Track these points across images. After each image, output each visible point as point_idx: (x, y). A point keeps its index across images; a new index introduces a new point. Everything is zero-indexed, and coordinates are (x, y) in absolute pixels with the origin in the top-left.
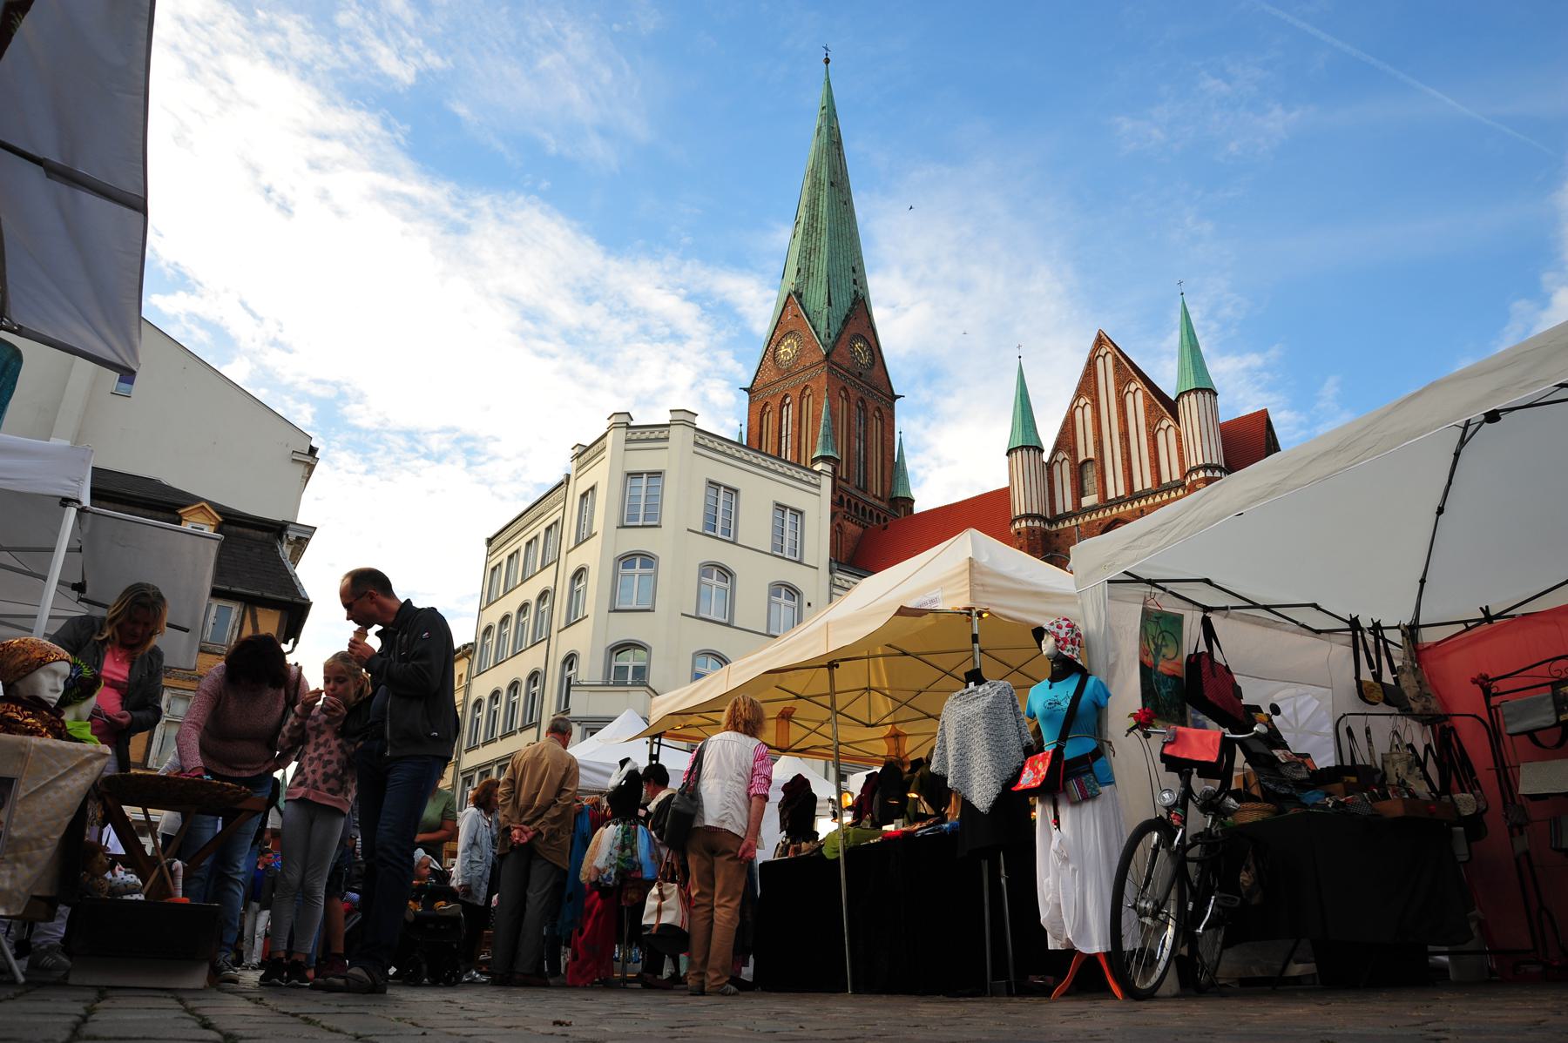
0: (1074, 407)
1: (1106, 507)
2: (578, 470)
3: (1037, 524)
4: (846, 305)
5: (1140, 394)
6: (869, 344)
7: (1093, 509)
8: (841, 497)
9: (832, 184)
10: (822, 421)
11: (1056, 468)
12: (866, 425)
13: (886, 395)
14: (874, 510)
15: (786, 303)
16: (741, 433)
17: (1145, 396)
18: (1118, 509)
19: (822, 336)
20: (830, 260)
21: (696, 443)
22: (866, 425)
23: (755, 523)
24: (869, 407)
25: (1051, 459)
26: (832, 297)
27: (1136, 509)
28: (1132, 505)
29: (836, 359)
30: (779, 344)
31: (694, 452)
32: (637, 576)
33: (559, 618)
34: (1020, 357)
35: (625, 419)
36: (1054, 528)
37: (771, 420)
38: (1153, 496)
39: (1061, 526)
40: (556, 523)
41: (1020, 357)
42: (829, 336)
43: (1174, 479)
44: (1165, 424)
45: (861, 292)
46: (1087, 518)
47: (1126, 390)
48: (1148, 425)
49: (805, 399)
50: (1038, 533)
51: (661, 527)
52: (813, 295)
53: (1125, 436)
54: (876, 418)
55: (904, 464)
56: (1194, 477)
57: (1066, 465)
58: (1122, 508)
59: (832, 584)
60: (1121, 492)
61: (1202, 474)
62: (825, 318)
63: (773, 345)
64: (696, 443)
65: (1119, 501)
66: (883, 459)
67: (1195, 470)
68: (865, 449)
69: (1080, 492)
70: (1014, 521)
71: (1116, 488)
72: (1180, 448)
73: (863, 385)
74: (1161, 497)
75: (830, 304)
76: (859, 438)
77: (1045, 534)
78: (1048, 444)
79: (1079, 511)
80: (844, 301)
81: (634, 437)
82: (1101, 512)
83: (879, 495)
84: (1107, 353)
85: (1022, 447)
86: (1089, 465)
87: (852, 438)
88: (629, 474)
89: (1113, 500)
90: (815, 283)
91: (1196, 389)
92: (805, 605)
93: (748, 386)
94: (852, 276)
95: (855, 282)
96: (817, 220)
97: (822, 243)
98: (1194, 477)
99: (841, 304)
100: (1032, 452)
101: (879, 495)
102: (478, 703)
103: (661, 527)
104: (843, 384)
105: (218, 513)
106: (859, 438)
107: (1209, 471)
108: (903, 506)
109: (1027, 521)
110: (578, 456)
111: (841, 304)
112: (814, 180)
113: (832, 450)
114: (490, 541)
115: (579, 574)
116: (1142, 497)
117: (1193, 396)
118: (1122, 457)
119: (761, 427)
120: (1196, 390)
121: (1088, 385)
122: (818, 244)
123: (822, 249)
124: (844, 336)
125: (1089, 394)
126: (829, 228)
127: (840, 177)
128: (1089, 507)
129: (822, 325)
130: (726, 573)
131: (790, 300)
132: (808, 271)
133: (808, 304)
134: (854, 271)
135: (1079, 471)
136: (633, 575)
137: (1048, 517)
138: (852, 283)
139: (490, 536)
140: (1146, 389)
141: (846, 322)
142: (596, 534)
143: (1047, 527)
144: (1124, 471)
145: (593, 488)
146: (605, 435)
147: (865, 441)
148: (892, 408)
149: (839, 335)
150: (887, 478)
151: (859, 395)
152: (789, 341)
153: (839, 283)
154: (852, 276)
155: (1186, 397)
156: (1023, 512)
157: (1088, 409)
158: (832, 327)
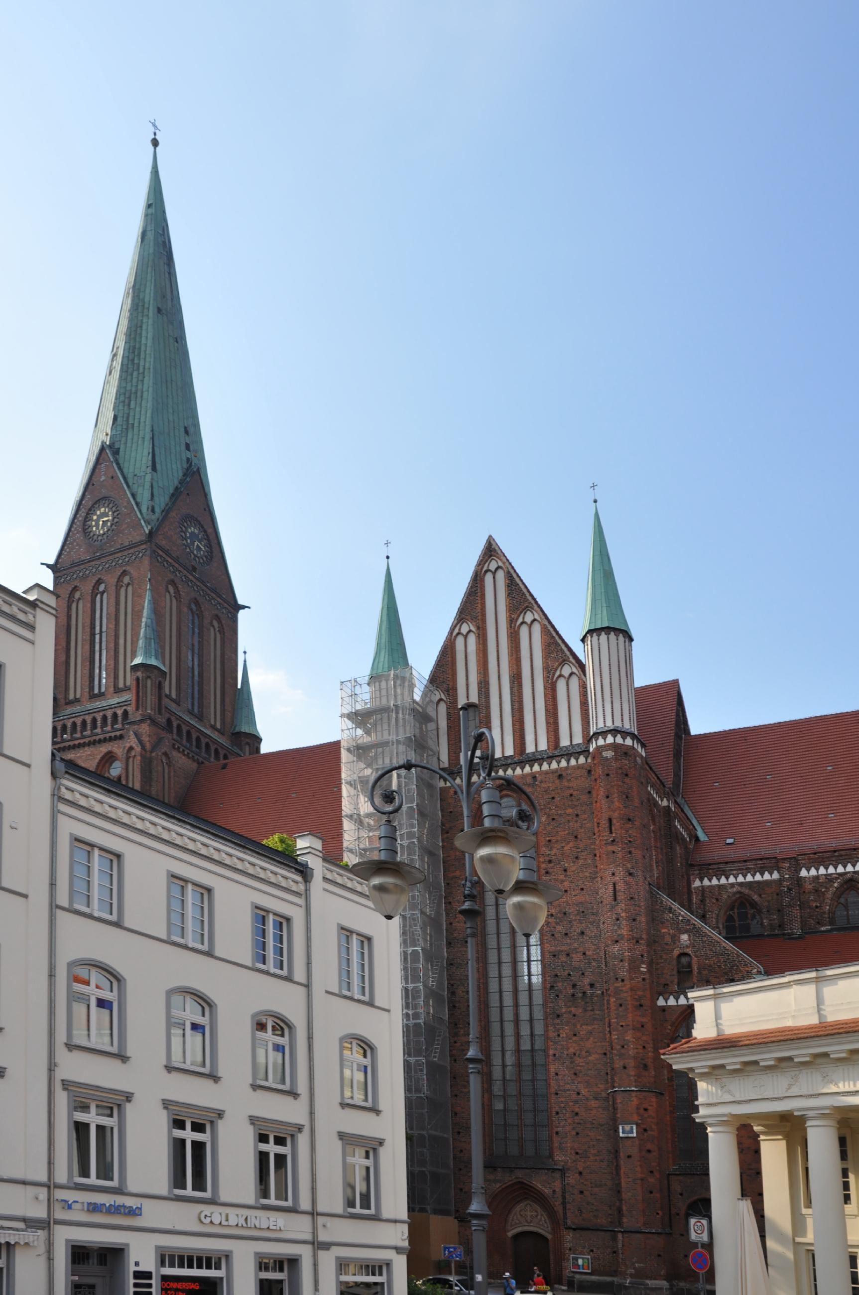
27: (527, 775)
38: (550, 760)
43: (574, 742)
44: (566, 671)
52: (133, 454)
67: (603, 734)
74: (559, 762)
75: (154, 468)
90: (136, 437)
107: (619, 736)
116: (535, 760)
118: (512, 705)
129: (144, 496)
131: (103, 455)
133: (126, 465)
144: (514, 725)
152: (102, 510)
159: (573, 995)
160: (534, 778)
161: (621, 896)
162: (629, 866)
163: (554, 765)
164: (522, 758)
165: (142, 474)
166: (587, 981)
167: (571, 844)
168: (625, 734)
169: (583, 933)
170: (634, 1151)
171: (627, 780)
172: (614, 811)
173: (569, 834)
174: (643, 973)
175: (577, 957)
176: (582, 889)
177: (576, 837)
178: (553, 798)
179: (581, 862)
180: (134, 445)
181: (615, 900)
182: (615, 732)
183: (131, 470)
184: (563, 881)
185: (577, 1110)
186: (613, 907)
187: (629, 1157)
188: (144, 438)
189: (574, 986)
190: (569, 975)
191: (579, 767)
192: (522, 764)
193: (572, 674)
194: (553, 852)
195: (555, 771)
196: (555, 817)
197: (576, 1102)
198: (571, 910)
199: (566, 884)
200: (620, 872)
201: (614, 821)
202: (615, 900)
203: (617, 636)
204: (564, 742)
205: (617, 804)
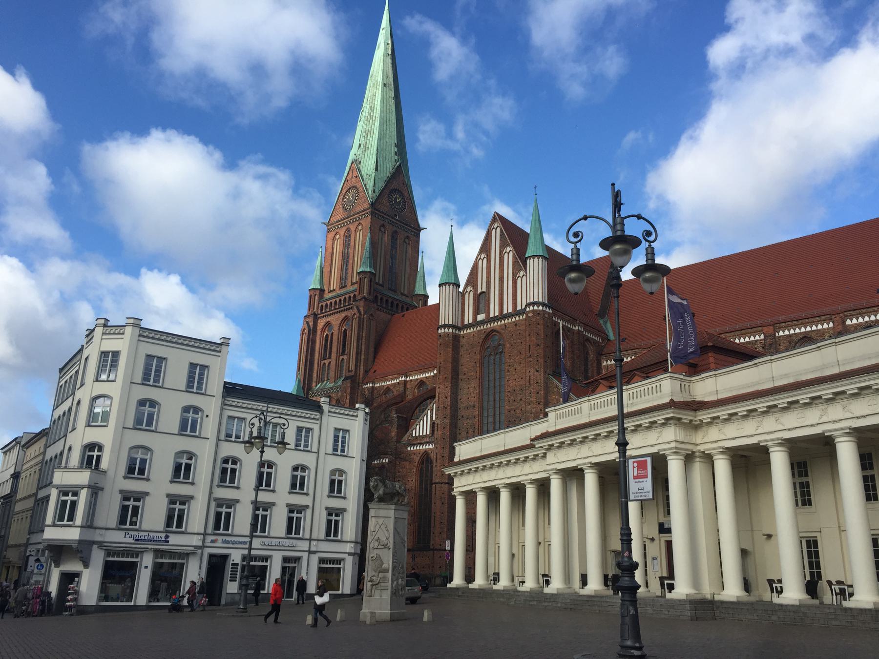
0: (478, 259)
4: (388, 170)
5: (511, 254)
7: (482, 323)
8: (376, 297)
9: (385, 85)
14: (399, 303)
17: (514, 256)
18: (494, 323)
19: (370, 192)
20: (379, 139)
25: (464, 290)
26: (378, 165)
28: (501, 322)
34: (452, 226)
36: (462, 333)
41: (452, 226)
44: (522, 273)
52: (367, 164)
54: (406, 243)
57: (472, 293)
62: (373, 179)
65: (495, 319)
71: (494, 311)
73: (398, 222)
74: (515, 318)
75: (377, 169)
78: (463, 281)
79: (476, 323)
80: (388, 168)
82: (485, 325)
90: (369, 154)
91: (534, 256)
92: (205, 416)
96: (374, 111)
99: (385, 169)
104: (383, 222)
111: (385, 169)
113: (370, 267)
116: (506, 318)
119: (333, 248)
122: (373, 128)
123: (375, 131)
132: (366, 146)
133: (363, 169)
137: (460, 325)
138: (393, 154)
140: (514, 252)
141: (389, 181)
143: (457, 332)
148: (418, 236)
153: (384, 155)
156: (443, 323)
157: (485, 260)
158: (376, 185)
160: (506, 326)
162: (537, 367)
163: (514, 319)
165: (371, 173)
167: (519, 357)
168: (543, 304)
169: (521, 399)
171: (539, 326)
172: (531, 342)
173: (518, 352)
175: (518, 411)
176: (522, 378)
177: (521, 353)
178: (512, 335)
179: (522, 365)
180: (368, 159)
181: (530, 384)
183: (366, 172)
184: (514, 375)
188: (373, 154)
190: (515, 420)
191: (523, 320)
194: (511, 361)
195: (514, 322)
196: (513, 344)
198: (517, 388)
199: (516, 376)
200: (533, 371)
201: (531, 346)
202: (530, 384)
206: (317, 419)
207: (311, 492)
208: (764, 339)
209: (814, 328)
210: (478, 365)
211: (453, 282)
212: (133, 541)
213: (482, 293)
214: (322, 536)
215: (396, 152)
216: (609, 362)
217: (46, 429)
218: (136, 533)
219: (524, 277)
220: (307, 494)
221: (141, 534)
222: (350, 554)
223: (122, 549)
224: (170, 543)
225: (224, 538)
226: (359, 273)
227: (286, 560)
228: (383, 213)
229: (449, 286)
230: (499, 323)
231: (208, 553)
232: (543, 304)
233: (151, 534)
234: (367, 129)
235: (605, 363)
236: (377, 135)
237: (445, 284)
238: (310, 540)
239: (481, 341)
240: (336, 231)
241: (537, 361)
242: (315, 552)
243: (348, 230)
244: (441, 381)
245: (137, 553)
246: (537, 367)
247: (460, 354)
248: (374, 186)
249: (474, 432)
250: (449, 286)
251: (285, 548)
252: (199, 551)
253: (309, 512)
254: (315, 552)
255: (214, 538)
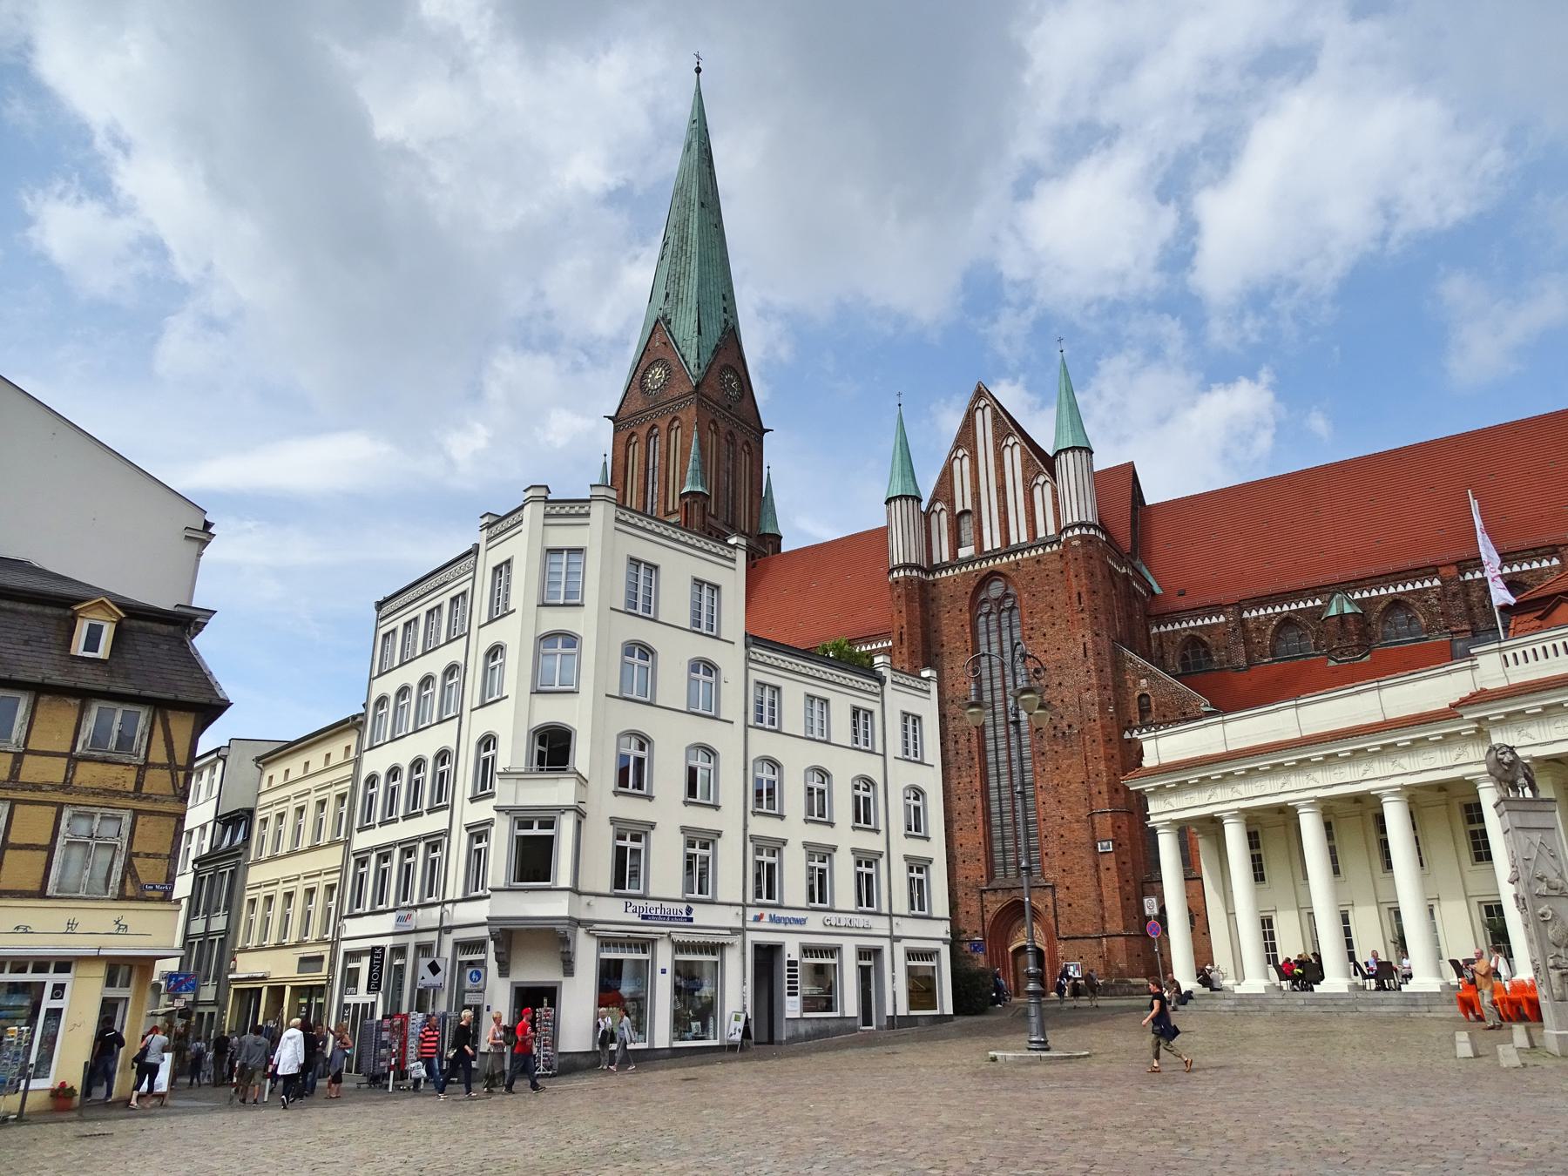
1: (983, 559)
2: (489, 540)
3: (915, 573)
5: (1017, 449)
6: (738, 376)
7: (970, 561)
9: (702, 205)
10: (692, 455)
11: (934, 517)
12: (734, 461)
13: (754, 429)
15: (653, 330)
16: (605, 463)
17: (1023, 451)
18: (994, 561)
19: (692, 367)
20: (700, 286)
21: (617, 520)
22: (734, 461)
23: (675, 600)
24: (739, 441)
25: (928, 508)
26: (702, 325)
27: (1011, 562)
28: (1008, 558)
29: (706, 391)
30: (646, 371)
31: (616, 529)
32: (559, 656)
33: (473, 695)
35: (542, 492)
36: (931, 577)
37: (636, 453)
39: (937, 576)
40: (464, 594)
42: (699, 367)
44: (1041, 479)
45: (731, 321)
46: (964, 569)
47: (1004, 444)
48: (1024, 479)
49: (673, 432)
50: (915, 582)
51: (583, 606)
52: (682, 322)
53: (1002, 489)
55: (772, 500)
56: (1070, 534)
57: (944, 515)
58: (998, 561)
59: (748, 659)
60: (997, 545)
61: (1077, 532)
63: (640, 373)
64: (617, 520)
65: (995, 554)
66: (751, 495)
67: (1072, 527)
68: (734, 484)
69: (956, 543)
70: (891, 571)
72: (1056, 504)
74: (1037, 551)
75: (699, 333)
76: (728, 473)
77: (923, 584)
79: (956, 562)
80: (714, 331)
81: (553, 512)
83: (747, 531)
84: (987, 405)
85: (900, 497)
86: (966, 518)
87: (721, 473)
88: (548, 550)
89: (989, 552)
93: (613, 414)
94: (722, 304)
95: (725, 310)
96: (687, 243)
97: (692, 268)
98: (1070, 534)
100: (910, 501)
101: (747, 531)
102: (372, 780)
103: (583, 606)
104: (712, 417)
105: (119, 607)
106: (728, 473)
108: (771, 542)
109: (905, 571)
110: (489, 526)
112: (684, 198)
114: (380, 605)
115: (495, 651)
116: (1018, 551)
117: (1070, 454)
119: (627, 457)
120: (1073, 449)
121: (966, 438)
124: (714, 367)
125: (967, 446)
126: (699, 253)
127: (710, 197)
128: (967, 558)
130: (646, 652)
134: (724, 298)
135: (956, 520)
136: (555, 654)
138: (722, 311)
139: (381, 599)
141: (717, 351)
142: (514, 611)
145: (508, 562)
146: (521, 508)
147: (734, 477)
149: (710, 366)
150: (755, 514)
151: (729, 428)
154: (722, 304)
155: (1063, 455)
156: (901, 562)
157: (966, 461)
158: (701, 357)
159: (1055, 735)
160: (1018, 564)
161: (1090, 653)
163: (1033, 553)
164: (1008, 549)
166: (1065, 723)
169: (1060, 684)
170: (1113, 864)
171: (1092, 562)
174: (1111, 713)
181: (1085, 656)
182: (1080, 525)
183: (681, 335)
184: (1043, 643)
185: (1062, 832)
186: (1084, 662)
187: (1108, 869)
189: (1055, 728)
191: (1053, 553)
192: (1007, 554)
193: (1046, 481)
195: (1035, 557)
197: (1061, 826)
199: (1046, 646)
201: (1083, 595)
202: (1085, 656)
203: (1081, 452)
204: (1041, 534)
205: (1084, 581)
206: (877, 694)
207: (882, 827)
208: (1443, 588)
209: (1526, 567)
210: (968, 630)
211: (913, 494)
212: (640, 920)
213: (965, 512)
214: (905, 910)
215: (725, 308)
216: (1162, 629)
217: (359, 715)
218: (641, 903)
219: (1047, 485)
220: (877, 831)
221: (652, 904)
222: (944, 941)
223: (626, 935)
224: (695, 923)
225: (773, 912)
226: (682, 496)
227: (863, 953)
228: (713, 402)
229: (907, 500)
230: (1005, 559)
231: (752, 942)
232: (1095, 527)
233: (666, 905)
234: (678, 270)
235: (1155, 630)
236: (696, 281)
237: (894, 498)
238: (891, 915)
239: (970, 590)
240: (631, 430)
241: (1096, 618)
242: (898, 939)
243: (654, 427)
244: (905, 657)
245: (646, 944)
246: (1095, 628)
247: (931, 613)
248: (698, 357)
249: (969, 740)
250: (907, 500)
251: (857, 931)
252: (740, 937)
253: (883, 862)
254: (898, 939)
255: (758, 911)
